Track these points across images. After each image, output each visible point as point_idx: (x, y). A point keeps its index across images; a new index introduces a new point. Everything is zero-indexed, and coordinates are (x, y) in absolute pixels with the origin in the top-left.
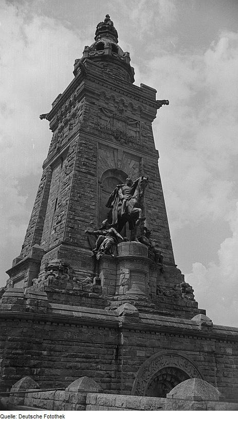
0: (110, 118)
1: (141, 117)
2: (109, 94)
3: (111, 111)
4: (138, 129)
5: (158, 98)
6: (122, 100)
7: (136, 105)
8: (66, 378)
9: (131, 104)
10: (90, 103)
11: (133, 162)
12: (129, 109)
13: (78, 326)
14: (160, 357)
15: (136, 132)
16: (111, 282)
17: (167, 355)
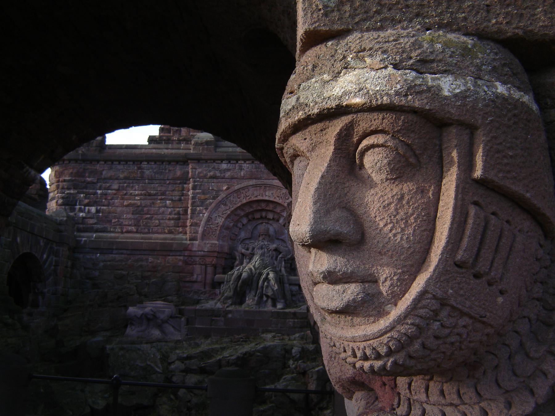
13: (136, 163)
14: (243, 188)
17: (252, 186)
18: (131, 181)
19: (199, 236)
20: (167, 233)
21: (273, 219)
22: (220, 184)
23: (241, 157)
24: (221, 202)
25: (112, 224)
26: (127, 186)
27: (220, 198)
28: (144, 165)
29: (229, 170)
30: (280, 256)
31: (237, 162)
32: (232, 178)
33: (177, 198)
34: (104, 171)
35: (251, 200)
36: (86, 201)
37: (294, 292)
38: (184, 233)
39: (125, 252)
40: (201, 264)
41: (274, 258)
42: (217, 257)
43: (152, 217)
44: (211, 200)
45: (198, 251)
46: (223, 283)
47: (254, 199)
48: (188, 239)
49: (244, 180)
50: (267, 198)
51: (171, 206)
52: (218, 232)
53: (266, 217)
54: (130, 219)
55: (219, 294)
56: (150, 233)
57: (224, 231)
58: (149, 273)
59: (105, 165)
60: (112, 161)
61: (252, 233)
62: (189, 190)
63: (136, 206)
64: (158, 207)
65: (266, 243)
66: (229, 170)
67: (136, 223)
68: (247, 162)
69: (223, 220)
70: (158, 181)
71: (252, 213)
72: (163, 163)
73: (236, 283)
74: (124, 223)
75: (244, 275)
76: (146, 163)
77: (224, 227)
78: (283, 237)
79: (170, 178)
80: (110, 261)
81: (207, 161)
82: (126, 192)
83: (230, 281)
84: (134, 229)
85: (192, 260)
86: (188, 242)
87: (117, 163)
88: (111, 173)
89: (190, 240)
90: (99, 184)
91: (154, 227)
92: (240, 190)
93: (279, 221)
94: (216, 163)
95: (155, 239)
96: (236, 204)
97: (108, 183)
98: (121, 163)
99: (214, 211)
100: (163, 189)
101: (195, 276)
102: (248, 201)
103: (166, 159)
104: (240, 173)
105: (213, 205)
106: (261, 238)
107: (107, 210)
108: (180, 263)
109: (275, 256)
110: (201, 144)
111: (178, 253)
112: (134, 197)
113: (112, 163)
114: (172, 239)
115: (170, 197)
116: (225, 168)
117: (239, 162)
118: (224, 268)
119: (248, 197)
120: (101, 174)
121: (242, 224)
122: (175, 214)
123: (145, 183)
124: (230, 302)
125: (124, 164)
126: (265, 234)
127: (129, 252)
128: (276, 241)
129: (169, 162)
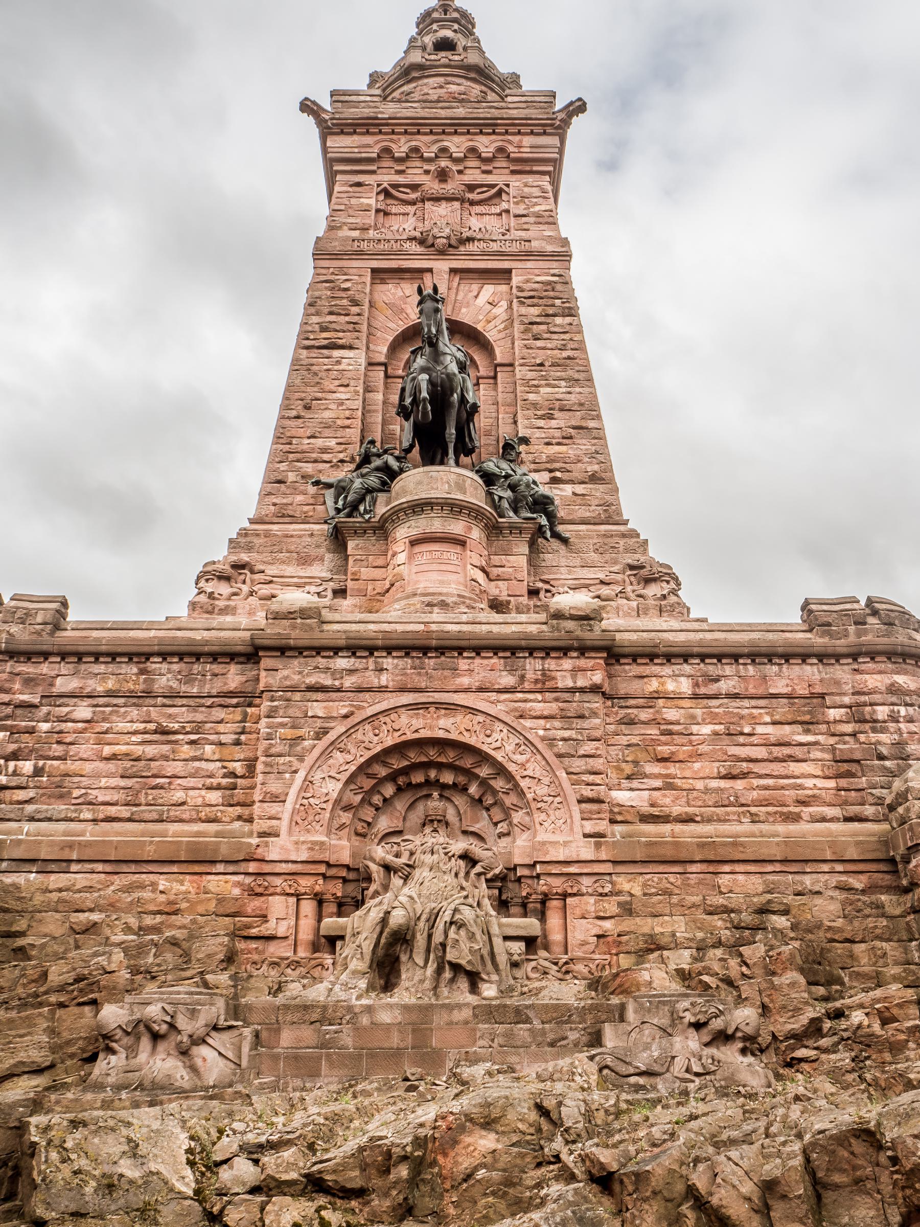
0: (413, 203)
1: (513, 172)
2: (401, 147)
3: (414, 187)
4: (504, 206)
5: (559, 105)
6: (444, 150)
7: (486, 145)
8: (104, 780)
9: (473, 150)
10: (351, 186)
11: (489, 291)
12: (475, 163)
13: (135, 660)
15: (500, 214)
16: (370, 588)
18: (121, 701)
19: (284, 825)
20: (203, 822)
21: (455, 784)
22: (331, 703)
23: (380, 643)
26: (111, 713)
27: (331, 736)
28: (155, 665)
29: (351, 672)
30: (478, 869)
31: (372, 654)
32: (360, 690)
33: (232, 737)
34: (59, 678)
35: (403, 738)
36: (12, 747)
37: (516, 957)
38: (246, 821)
39: (100, 867)
40: (288, 894)
41: (462, 874)
42: (324, 876)
44: (311, 742)
45: (280, 862)
46: (342, 938)
47: (410, 736)
48: (255, 835)
49: (390, 695)
50: (441, 734)
51: (216, 757)
52: (328, 815)
53: (438, 780)
55: (331, 967)
56: (162, 821)
57: (341, 813)
58: (159, 918)
59: (62, 664)
60: (80, 656)
61: (404, 819)
62: (260, 719)
64: (184, 760)
65: (441, 840)
66: (351, 672)
67: (129, 798)
68: (394, 654)
69: (340, 785)
70: (185, 701)
71: (405, 771)
72: (198, 659)
73: (375, 936)
74: (100, 799)
75: (398, 918)
76: (160, 660)
77: (341, 805)
78: (478, 826)
79: (214, 692)
80: (60, 890)
81: (301, 653)
82: (108, 725)
83: (358, 933)
84: (125, 812)
85: (266, 883)
86: (255, 841)
87: (92, 659)
90: (45, 709)
91: (173, 808)
92: (380, 716)
93: (467, 789)
94: (323, 657)
96: (369, 749)
97: (67, 705)
98: (101, 659)
99: (317, 765)
100: (199, 717)
101: (272, 923)
102: (398, 740)
103: (206, 649)
104: (379, 679)
105: (316, 752)
106: (428, 830)
107: (62, 767)
108: (236, 891)
109: (463, 870)
110: (289, 615)
111: (231, 869)
113: (80, 659)
114: (217, 834)
115: (213, 737)
116: (344, 666)
117: (376, 654)
118: (340, 905)
120: (52, 685)
121: (381, 799)
123: (154, 706)
124: (363, 984)
126: (438, 818)
127: (108, 868)
128: (461, 837)
129: (215, 657)
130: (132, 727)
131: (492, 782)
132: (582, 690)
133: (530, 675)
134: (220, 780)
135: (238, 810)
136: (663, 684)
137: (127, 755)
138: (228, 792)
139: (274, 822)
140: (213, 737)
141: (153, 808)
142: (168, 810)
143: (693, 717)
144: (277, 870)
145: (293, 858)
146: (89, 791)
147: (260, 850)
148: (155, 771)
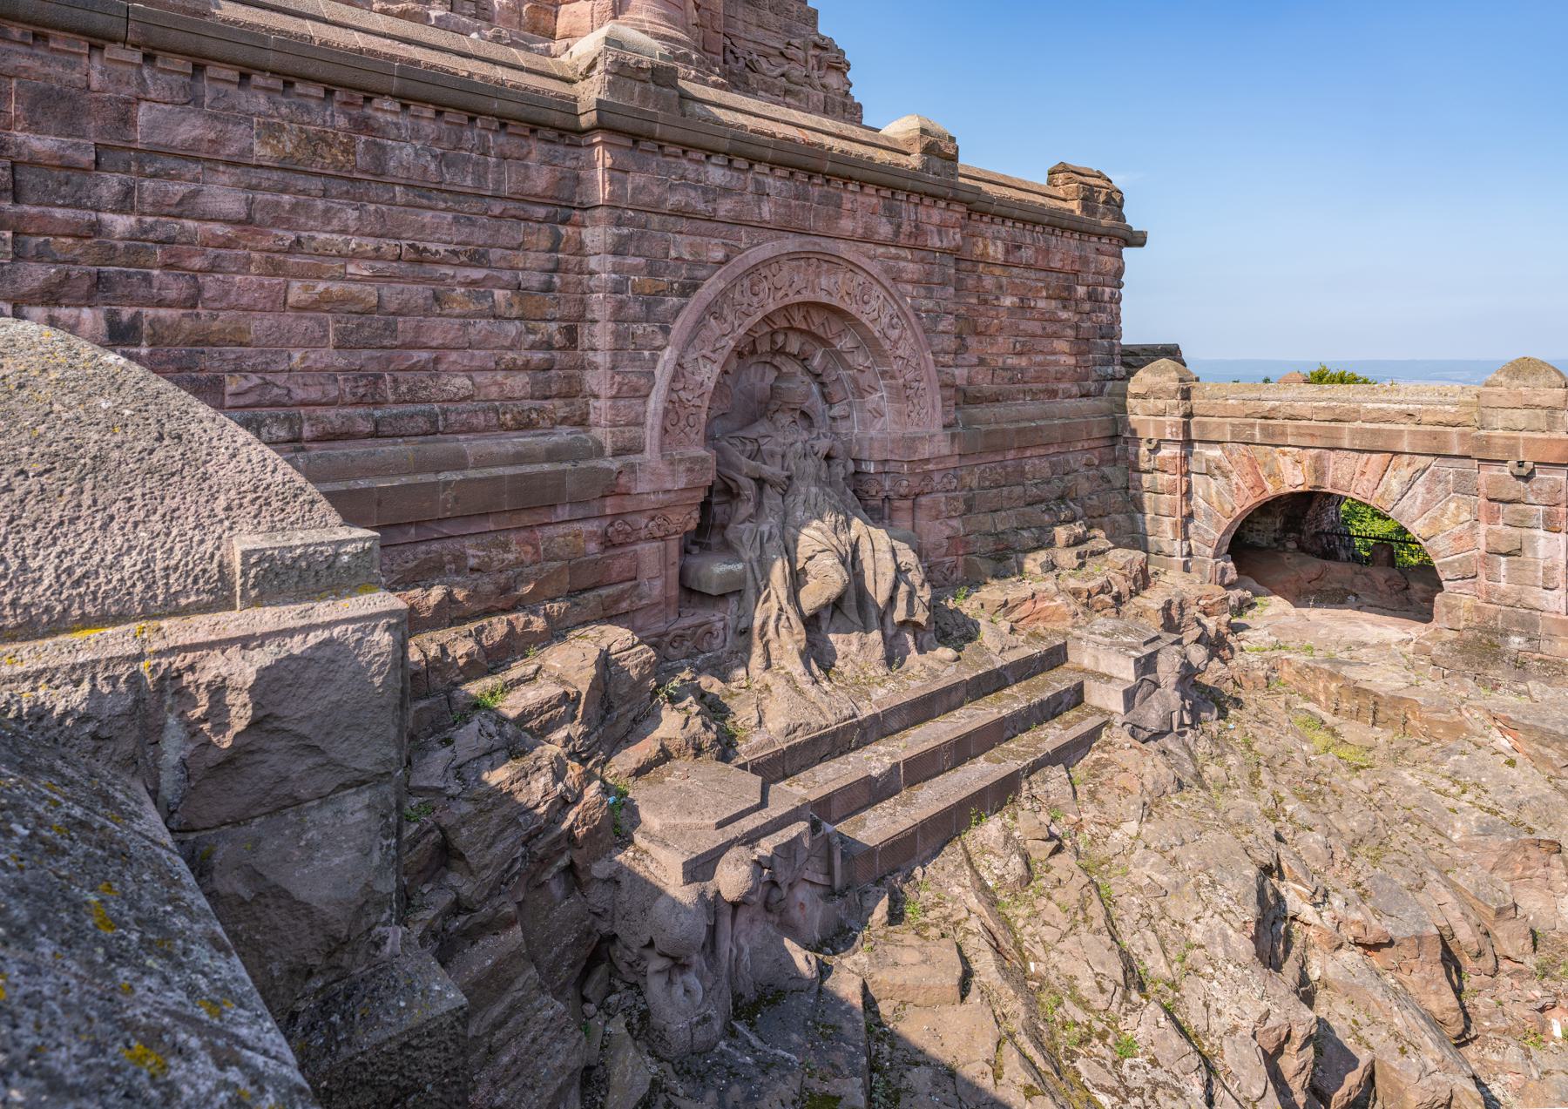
14: (766, 263)
17: (793, 256)
18: (316, 185)
19: (651, 434)
22: (698, 239)
24: (713, 310)
25: (228, 401)
26: (294, 208)
35: (787, 301)
43: (437, 361)
50: (824, 299)
51: (515, 312)
54: (330, 374)
63: (358, 308)
84: (360, 419)
86: (615, 464)
88: (190, 129)
89: (617, 453)
91: (451, 406)
95: (481, 462)
112: (338, 263)
114: (553, 455)
119: (781, 294)
122: (532, 347)
123: (392, 202)
125: (267, 89)
130: (347, 243)
131: (848, 357)
132: (943, 252)
133: (906, 228)
134: (529, 354)
135: (559, 407)
136: (986, 247)
137: (345, 300)
138: (541, 376)
139: (632, 432)
140: (507, 276)
141: (410, 408)
142: (445, 412)
143: (1001, 287)
144: (645, 506)
145: (668, 486)
146: (268, 377)
147: (623, 480)
148: (409, 337)
